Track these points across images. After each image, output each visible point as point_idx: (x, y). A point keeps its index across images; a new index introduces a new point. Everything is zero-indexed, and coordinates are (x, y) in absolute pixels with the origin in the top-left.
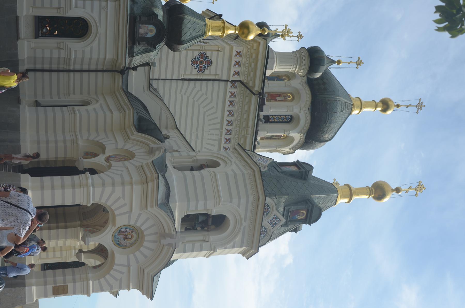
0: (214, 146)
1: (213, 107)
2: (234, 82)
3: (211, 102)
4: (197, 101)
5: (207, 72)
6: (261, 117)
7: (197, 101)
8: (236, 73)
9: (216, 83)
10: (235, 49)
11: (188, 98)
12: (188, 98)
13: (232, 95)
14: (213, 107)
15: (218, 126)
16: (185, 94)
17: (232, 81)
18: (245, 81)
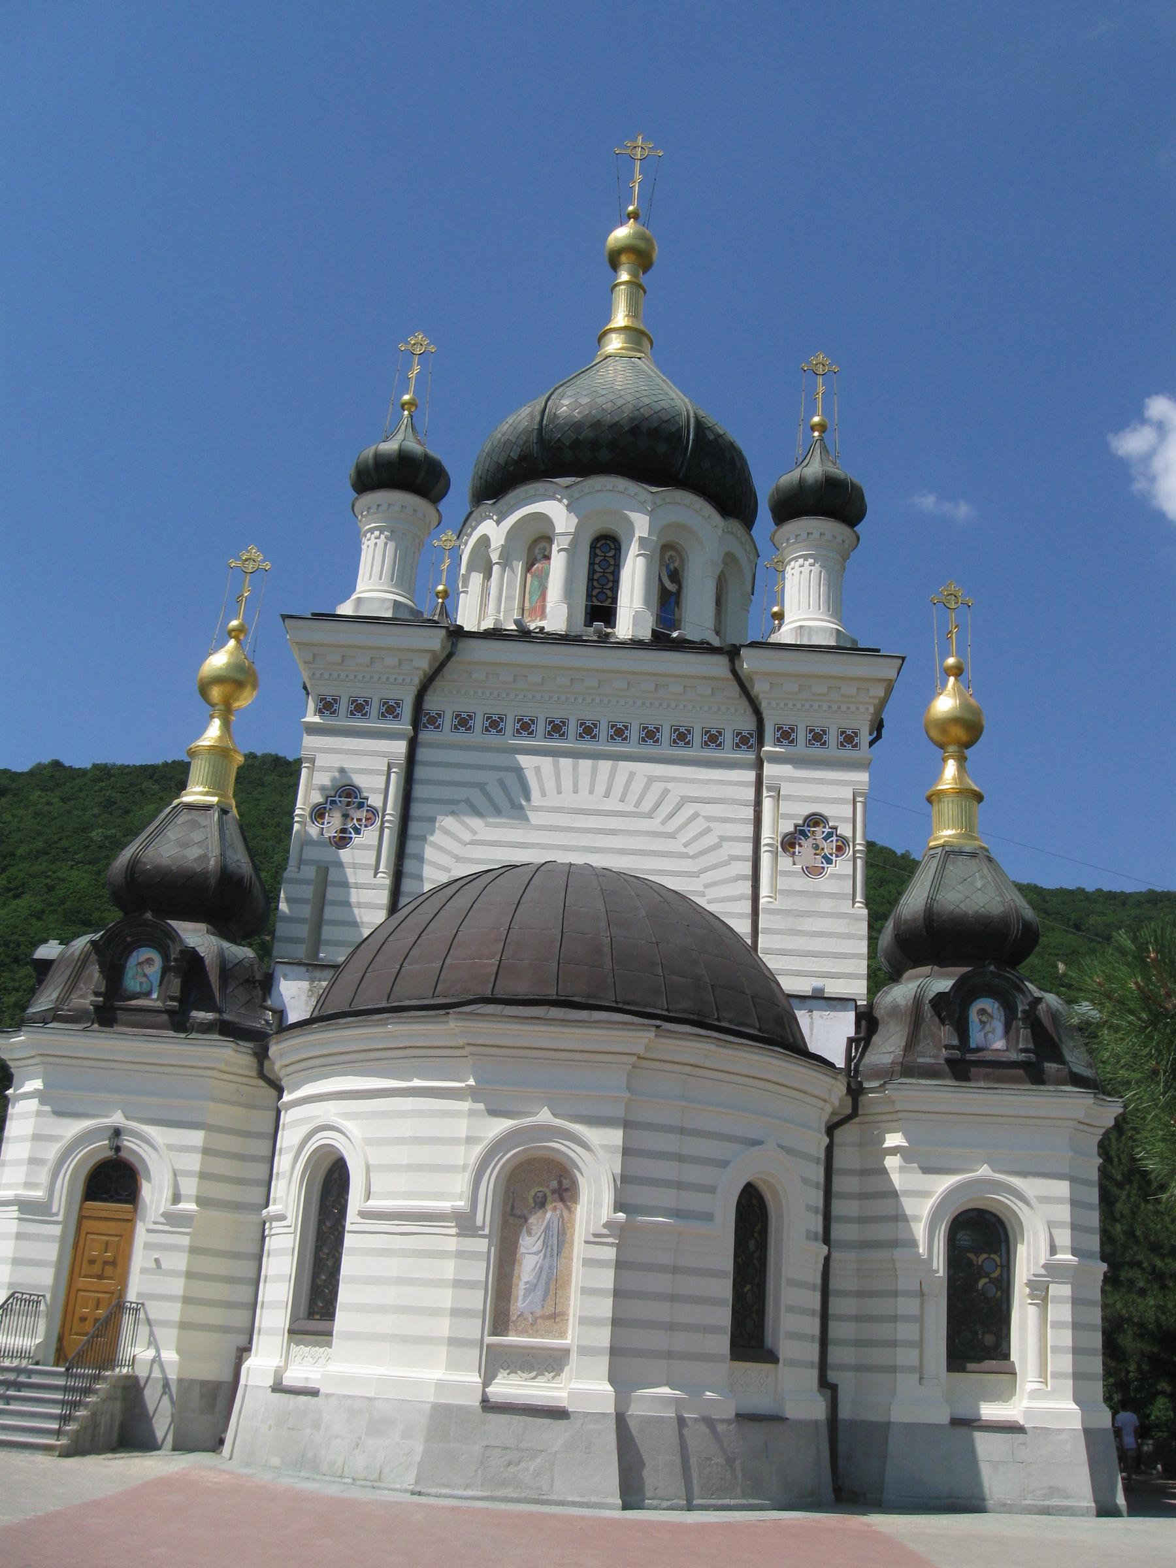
0: (632, 775)
1: (501, 782)
2: (425, 720)
3: (482, 787)
4: (475, 833)
5: (375, 801)
6: (590, 633)
7: (475, 833)
8: (390, 710)
9: (420, 772)
10: (312, 718)
11: (458, 859)
12: (458, 859)
13: (463, 722)
14: (501, 782)
15: (566, 763)
16: (448, 870)
17: (416, 724)
18: (416, 681)
